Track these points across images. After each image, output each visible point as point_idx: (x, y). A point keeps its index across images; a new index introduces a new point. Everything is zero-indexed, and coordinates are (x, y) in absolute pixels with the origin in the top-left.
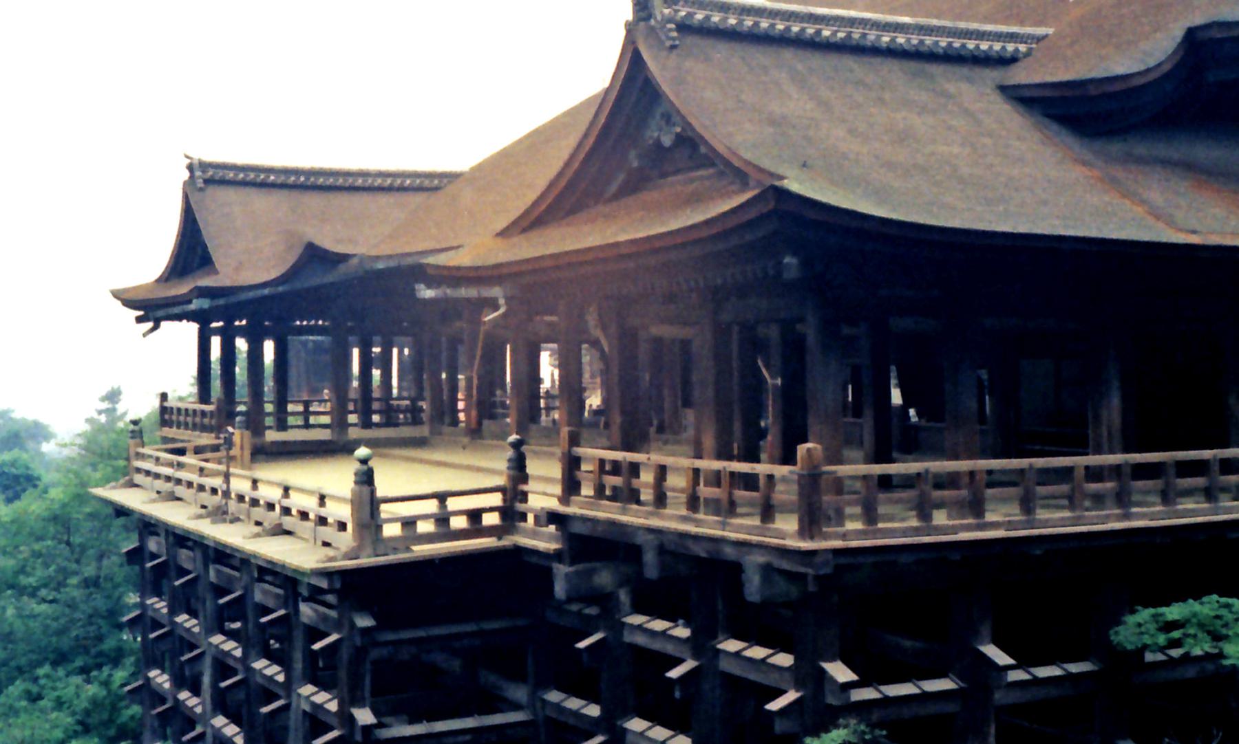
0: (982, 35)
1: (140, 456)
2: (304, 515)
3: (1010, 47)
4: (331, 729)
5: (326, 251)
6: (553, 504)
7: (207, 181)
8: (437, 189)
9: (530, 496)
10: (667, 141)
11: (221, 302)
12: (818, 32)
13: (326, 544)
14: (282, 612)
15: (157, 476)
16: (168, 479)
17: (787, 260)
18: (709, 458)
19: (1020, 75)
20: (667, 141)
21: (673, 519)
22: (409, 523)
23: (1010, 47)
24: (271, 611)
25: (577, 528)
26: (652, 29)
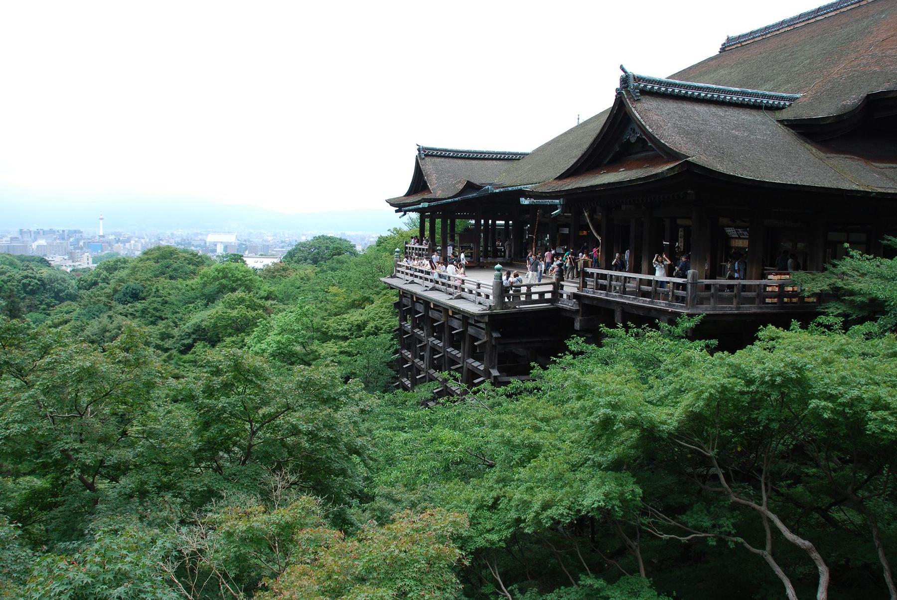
0: (770, 97)
1: (400, 266)
2: (471, 292)
3: (782, 103)
4: (481, 377)
6: (575, 290)
10: (633, 140)
11: (432, 204)
12: (699, 94)
13: (480, 303)
15: (407, 274)
16: (411, 275)
19: (785, 115)
20: (633, 140)
21: (629, 300)
23: (782, 103)
25: (586, 302)
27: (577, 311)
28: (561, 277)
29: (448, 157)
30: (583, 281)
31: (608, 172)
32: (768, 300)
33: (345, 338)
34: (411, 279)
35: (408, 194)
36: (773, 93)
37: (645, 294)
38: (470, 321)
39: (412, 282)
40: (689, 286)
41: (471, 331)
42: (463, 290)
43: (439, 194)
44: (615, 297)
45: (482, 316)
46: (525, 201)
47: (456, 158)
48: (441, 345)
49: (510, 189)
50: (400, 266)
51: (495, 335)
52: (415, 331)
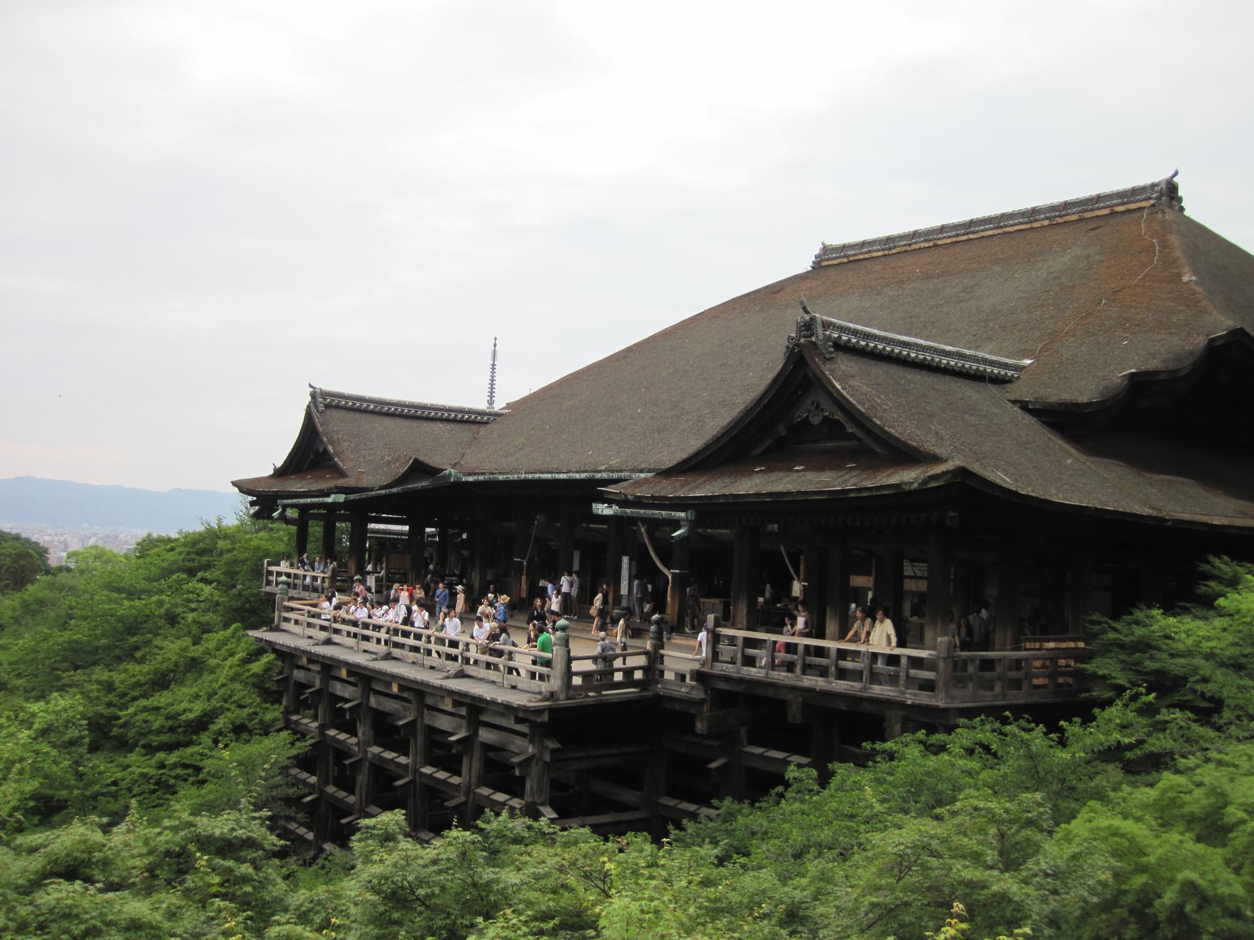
0: (992, 363)
1: (292, 609)
5: (427, 466)
6: (696, 666)
8: (486, 423)
10: (816, 421)
11: (352, 497)
13: (514, 687)
15: (309, 625)
17: (952, 514)
18: (833, 639)
20: (816, 421)
21: (819, 683)
24: (452, 734)
25: (722, 686)
26: (814, 344)
27: (702, 701)
28: (659, 645)
29: (366, 411)
31: (769, 470)
32: (1035, 682)
33: (170, 748)
34: (323, 635)
35: (280, 473)
36: (994, 358)
37: (842, 674)
38: (485, 718)
39: (328, 642)
40: (941, 665)
41: (485, 735)
42: (467, 661)
43: (365, 482)
44: (781, 676)
45: (539, 711)
46: (601, 509)
47: (380, 413)
48: (403, 760)
49: (501, 477)
51: (552, 745)
52: (332, 732)
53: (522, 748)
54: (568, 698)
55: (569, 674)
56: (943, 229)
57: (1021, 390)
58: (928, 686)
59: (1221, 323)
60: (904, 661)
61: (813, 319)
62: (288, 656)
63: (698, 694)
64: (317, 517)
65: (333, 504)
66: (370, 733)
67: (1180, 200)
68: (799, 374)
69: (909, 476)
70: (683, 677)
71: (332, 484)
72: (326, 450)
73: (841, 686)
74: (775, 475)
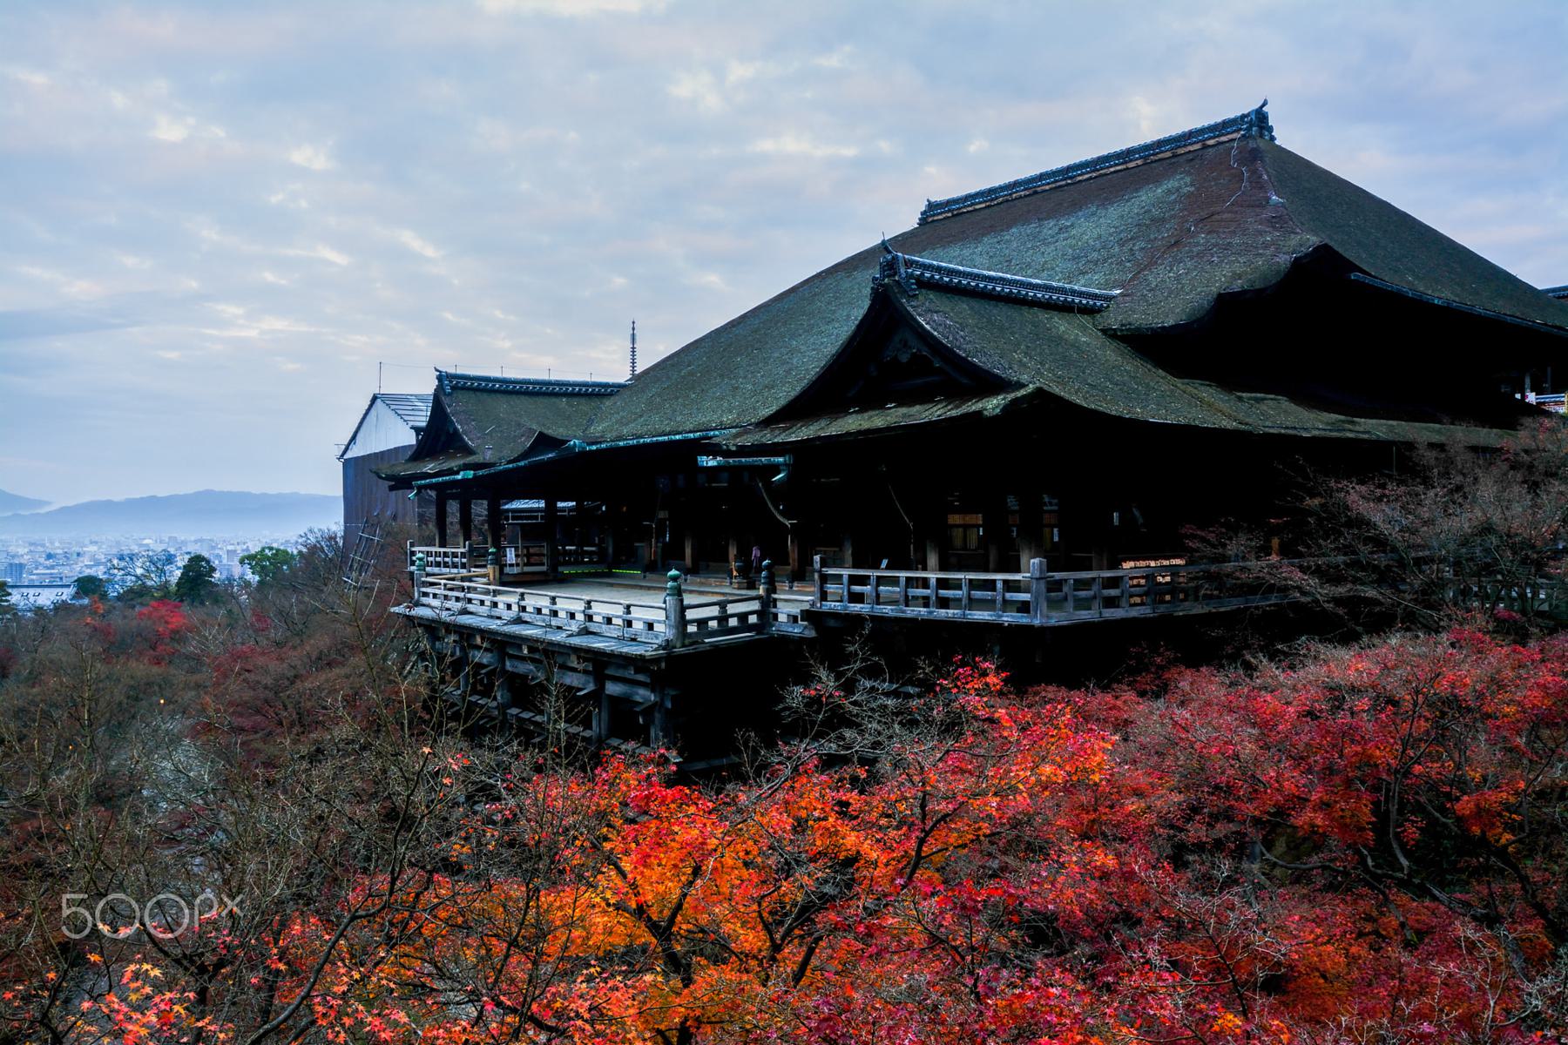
0: (1081, 294)
1: (425, 584)
6: (806, 607)
7: (453, 388)
8: (611, 394)
9: (779, 604)
10: (904, 358)
11: (480, 473)
13: (634, 640)
14: (591, 687)
15: (446, 597)
18: (933, 571)
20: (904, 358)
21: (920, 612)
22: (702, 623)
24: (581, 690)
25: (832, 623)
28: (772, 589)
30: (822, 588)
37: (944, 603)
38: (610, 672)
39: (464, 612)
41: (612, 689)
46: (708, 462)
50: (425, 584)
53: (644, 695)
54: (684, 646)
55: (683, 622)
56: (1042, 177)
57: (1113, 320)
58: (1024, 607)
59: (1307, 239)
60: (999, 585)
61: (895, 258)
62: (433, 628)
63: (811, 634)
64: (453, 497)
65: (463, 480)
66: (508, 695)
67: (1270, 129)
68: (886, 315)
69: (992, 405)
70: (795, 619)
71: (461, 462)
72: (456, 430)
73: (942, 613)
74: (866, 415)
